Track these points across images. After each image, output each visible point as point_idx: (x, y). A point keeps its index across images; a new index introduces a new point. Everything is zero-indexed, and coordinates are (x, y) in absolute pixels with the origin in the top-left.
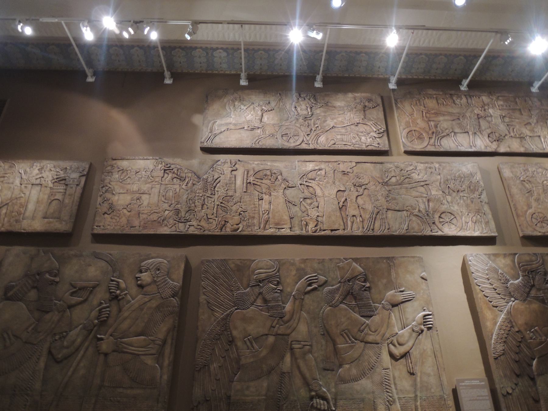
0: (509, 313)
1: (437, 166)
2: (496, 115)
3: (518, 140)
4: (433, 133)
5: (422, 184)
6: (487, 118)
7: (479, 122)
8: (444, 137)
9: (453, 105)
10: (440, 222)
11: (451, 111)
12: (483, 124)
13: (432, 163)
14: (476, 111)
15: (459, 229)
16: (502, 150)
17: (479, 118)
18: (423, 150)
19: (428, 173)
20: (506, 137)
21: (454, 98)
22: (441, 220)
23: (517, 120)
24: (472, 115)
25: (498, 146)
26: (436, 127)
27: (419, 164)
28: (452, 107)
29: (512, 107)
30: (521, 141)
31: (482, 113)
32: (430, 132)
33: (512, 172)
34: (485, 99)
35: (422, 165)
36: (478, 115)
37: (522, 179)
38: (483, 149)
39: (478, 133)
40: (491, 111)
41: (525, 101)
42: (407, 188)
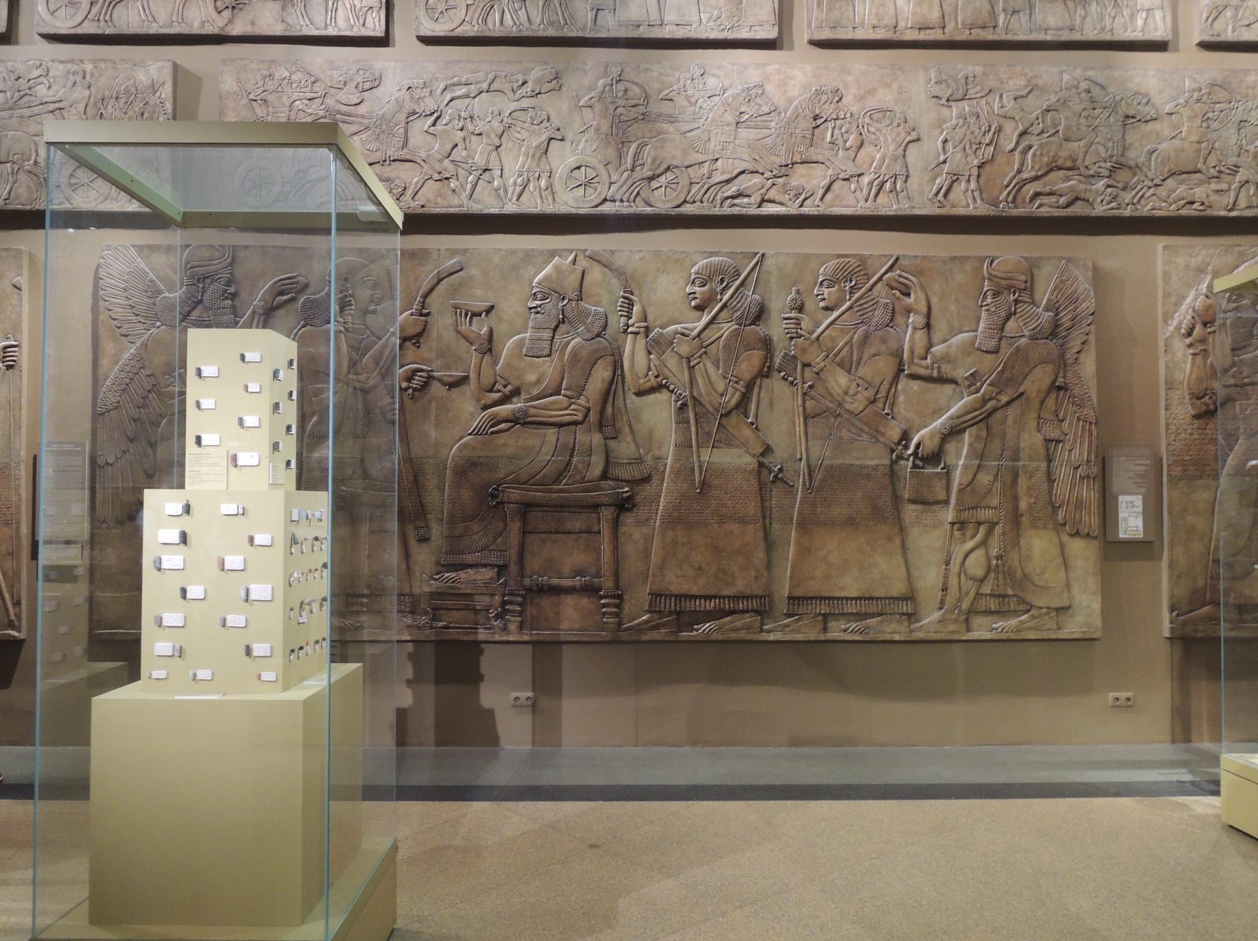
0: (145, 345)
1: (89, 67)
5: (51, 107)
10: (71, 185)
13: (82, 61)
15: (101, 199)
16: (236, 30)
18: (73, 31)
19: (69, 84)
22: (73, 181)
25: (231, 21)
27: (55, 64)
30: (283, 8)
33: (239, 81)
35: (61, 66)
37: (251, 97)
38: (196, 29)
42: (22, 117)
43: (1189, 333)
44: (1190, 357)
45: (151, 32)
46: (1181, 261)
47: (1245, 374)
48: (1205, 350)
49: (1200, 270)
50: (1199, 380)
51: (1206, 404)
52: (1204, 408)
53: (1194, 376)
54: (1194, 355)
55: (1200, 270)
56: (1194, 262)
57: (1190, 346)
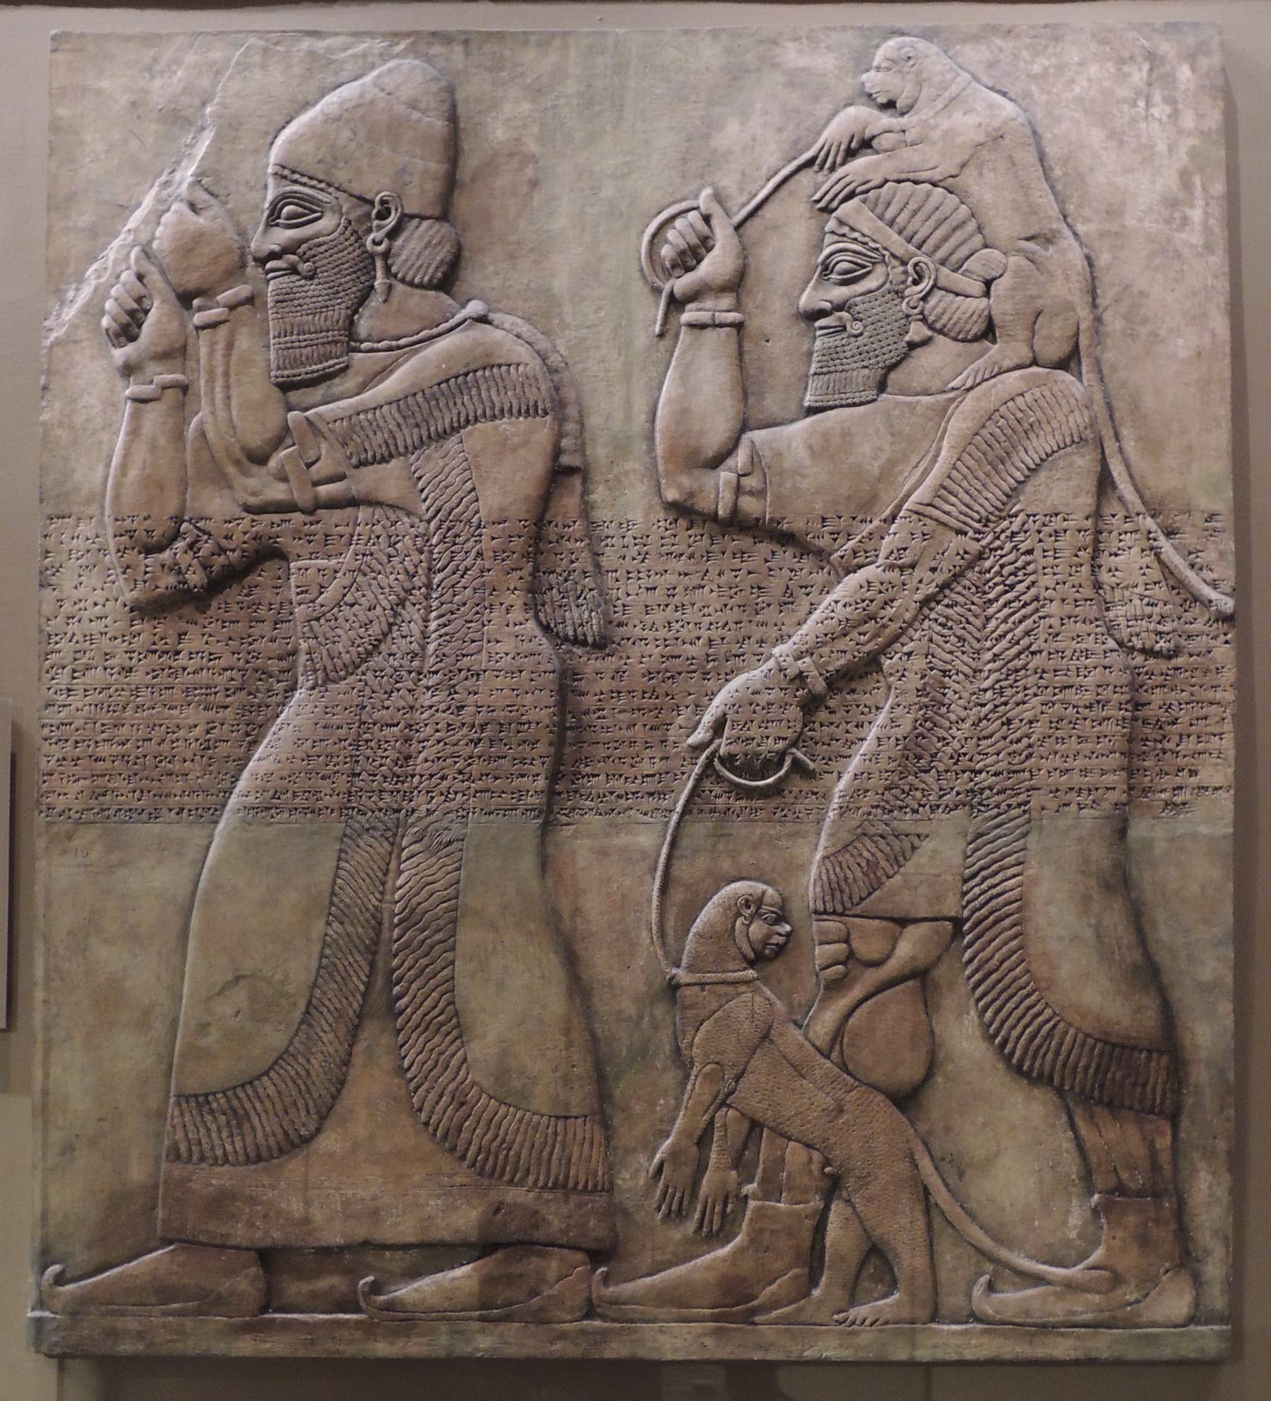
43: (127, 331)
44: (129, 407)
46: (115, 85)
47: (319, 470)
48: (184, 388)
49: (179, 119)
50: (153, 484)
51: (175, 569)
52: (171, 580)
53: (133, 473)
54: (140, 401)
55: (179, 119)
56: (163, 89)
57: (128, 370)
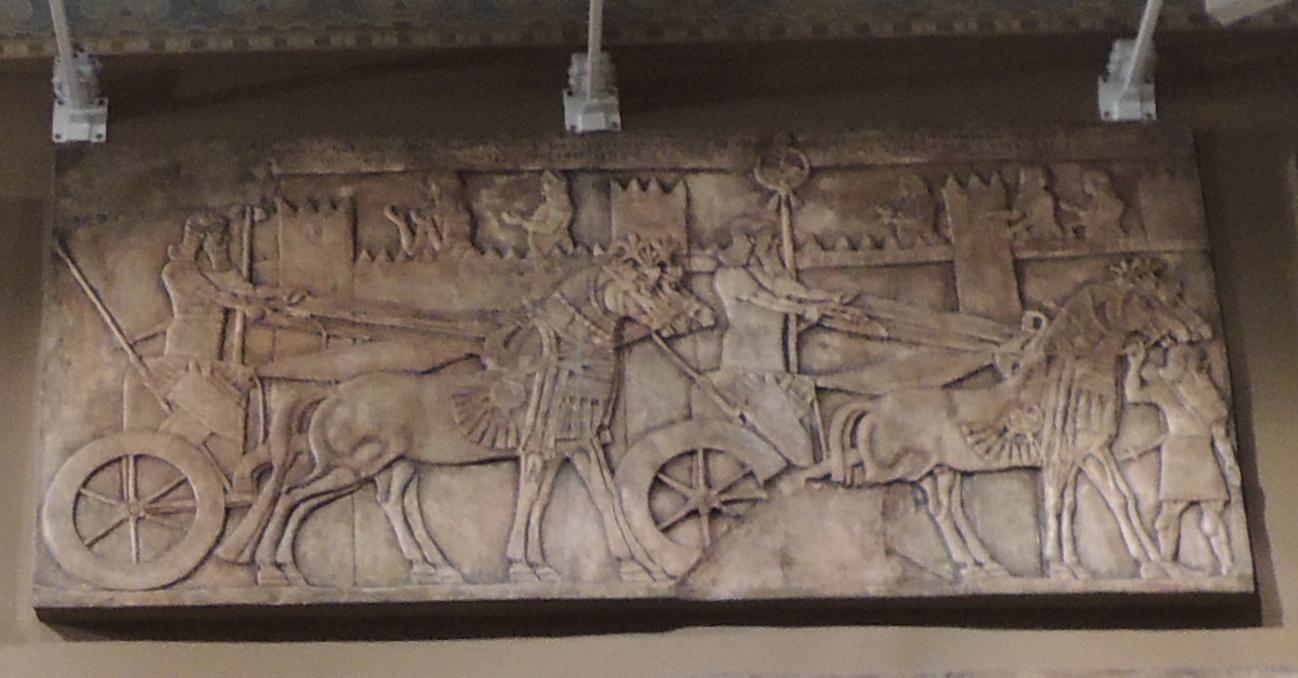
2: (754, 320)
3: (867, 504)
4: (262, 472)
6: (684, 346)
7: (618, 380)
8: (335, 495)
9: (466, 255)
11: (431, 303)
12: (650, 387)
14: (622, 293)
16: (729, 583)
17: (621, 348)
18: (162, 599)
20: (785, 486)
21: (485, 200)
23: (903, 353)
24: (582, 326)
25: (708, 555)
26: (297, 422)
28: (451, 271)
29: (891, 252)
30: (887, 512)
31: (652, 310)
32: (245, 467)
34: (713, 196)
36: (625, 320)
38: (591, 584)
39: (589, 468)
40: (728, 287)
41: (1010, 194)
45: (437, 594)
